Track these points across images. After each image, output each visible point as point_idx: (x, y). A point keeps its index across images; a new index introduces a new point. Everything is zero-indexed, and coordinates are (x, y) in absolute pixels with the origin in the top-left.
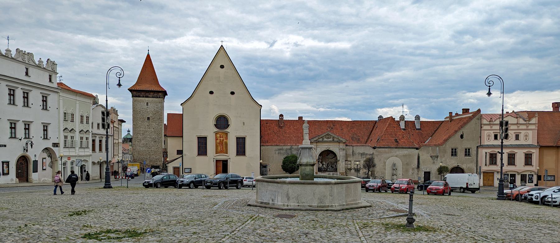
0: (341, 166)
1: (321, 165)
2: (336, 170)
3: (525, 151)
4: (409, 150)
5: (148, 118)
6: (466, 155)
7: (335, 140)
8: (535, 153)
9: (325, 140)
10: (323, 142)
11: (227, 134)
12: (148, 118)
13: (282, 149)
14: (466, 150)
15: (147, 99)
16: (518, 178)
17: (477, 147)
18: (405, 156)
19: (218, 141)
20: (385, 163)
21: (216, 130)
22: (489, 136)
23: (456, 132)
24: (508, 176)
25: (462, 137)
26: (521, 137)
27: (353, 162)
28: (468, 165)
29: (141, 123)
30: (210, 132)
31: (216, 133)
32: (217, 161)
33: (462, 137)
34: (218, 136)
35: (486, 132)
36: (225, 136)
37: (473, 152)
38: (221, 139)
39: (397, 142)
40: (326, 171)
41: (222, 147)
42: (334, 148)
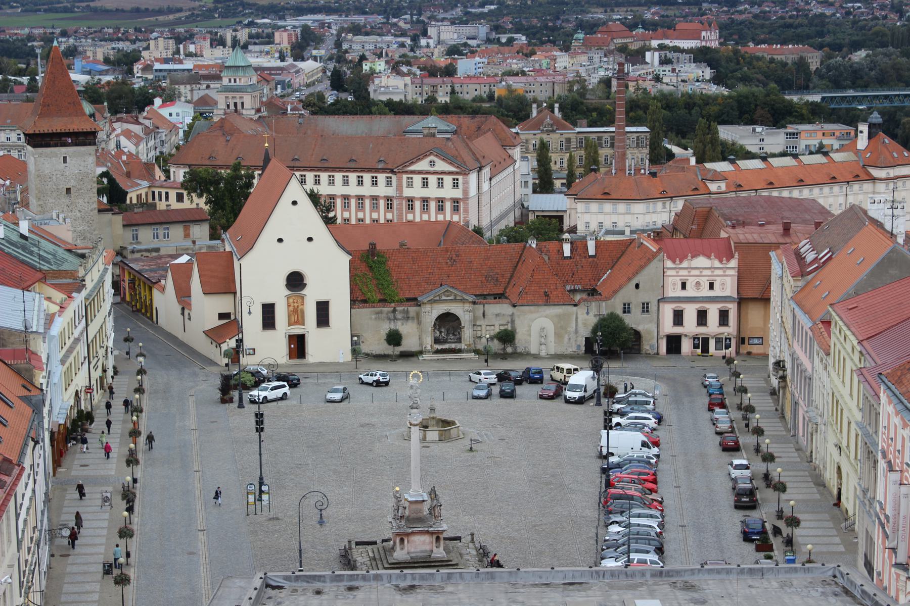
0: (467, 334)
1: (438, 334)
2: (459, 340)
3: (720, 306)
4: (564, 307)
5: (68, 190)
6: (643, 311)
7: (458, 298)
8: (732, 308)
9: (444, 298)
10: (440, 301)
11: (302, 298)
12: (68, 190)
13: (381, 312)
14: (643, 304)
15: (63, 150)
16: (712, 343)
17: (658, 300)
18: (559, 316)
19: (291, 308)
20: (530, 326)
21: (288, 292)
22: (674, 284)
23: (630, 279)
24: (699, 340)
25: (637, 286)
26: (716, 286)
27: (484, 327)
28: (647, 326)
29: (54, 201)
30: (279, 295)
31: (288, 297)
32: (291, 338)
33: (637, 286)
34: (291, 300)
35: (670, 279)
36: (300, 300)
37: (653, 307)
38: (296, 305)
39: (548, 296)
40: (445, 342)
41: (297, 316)
42: (456, 309)
